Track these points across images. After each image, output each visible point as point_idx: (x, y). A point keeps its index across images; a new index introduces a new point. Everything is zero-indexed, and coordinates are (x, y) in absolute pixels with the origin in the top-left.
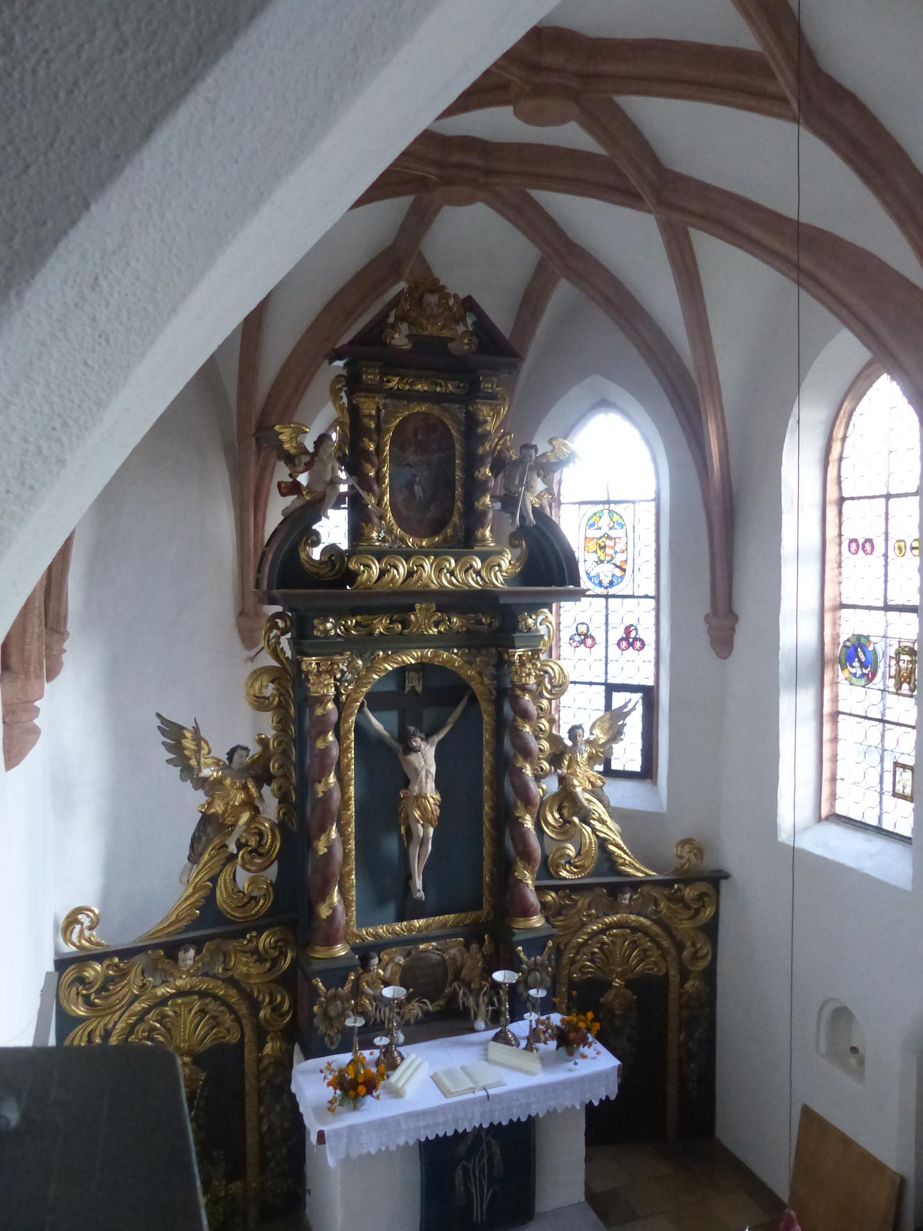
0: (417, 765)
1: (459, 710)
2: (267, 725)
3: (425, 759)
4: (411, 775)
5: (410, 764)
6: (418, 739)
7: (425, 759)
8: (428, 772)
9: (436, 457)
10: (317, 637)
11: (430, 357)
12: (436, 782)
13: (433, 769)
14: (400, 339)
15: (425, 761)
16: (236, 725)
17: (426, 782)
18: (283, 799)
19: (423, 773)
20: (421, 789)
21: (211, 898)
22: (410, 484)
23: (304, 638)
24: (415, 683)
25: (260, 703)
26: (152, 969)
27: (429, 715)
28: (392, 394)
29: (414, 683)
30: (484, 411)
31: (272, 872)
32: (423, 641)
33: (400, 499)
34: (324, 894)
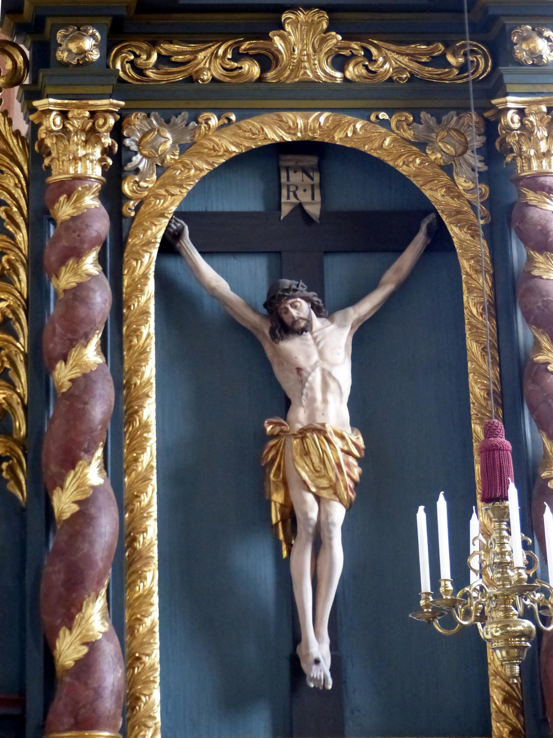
0: (302, 361)
1: (408, 258)
3: (324, 357)
4: (287, 382)
5: (286, 360)
6: (305, 306)
7: (324, 357)
8: (326, 376)
10: (65, 65)
12: (352, 404)
15: (321, 353)
17: (325, 401)
19: (316, 379)
20: (311, 415)
24: (304, 197)
27: (338, 269)
29: (301, 192)
32: (310, 95)
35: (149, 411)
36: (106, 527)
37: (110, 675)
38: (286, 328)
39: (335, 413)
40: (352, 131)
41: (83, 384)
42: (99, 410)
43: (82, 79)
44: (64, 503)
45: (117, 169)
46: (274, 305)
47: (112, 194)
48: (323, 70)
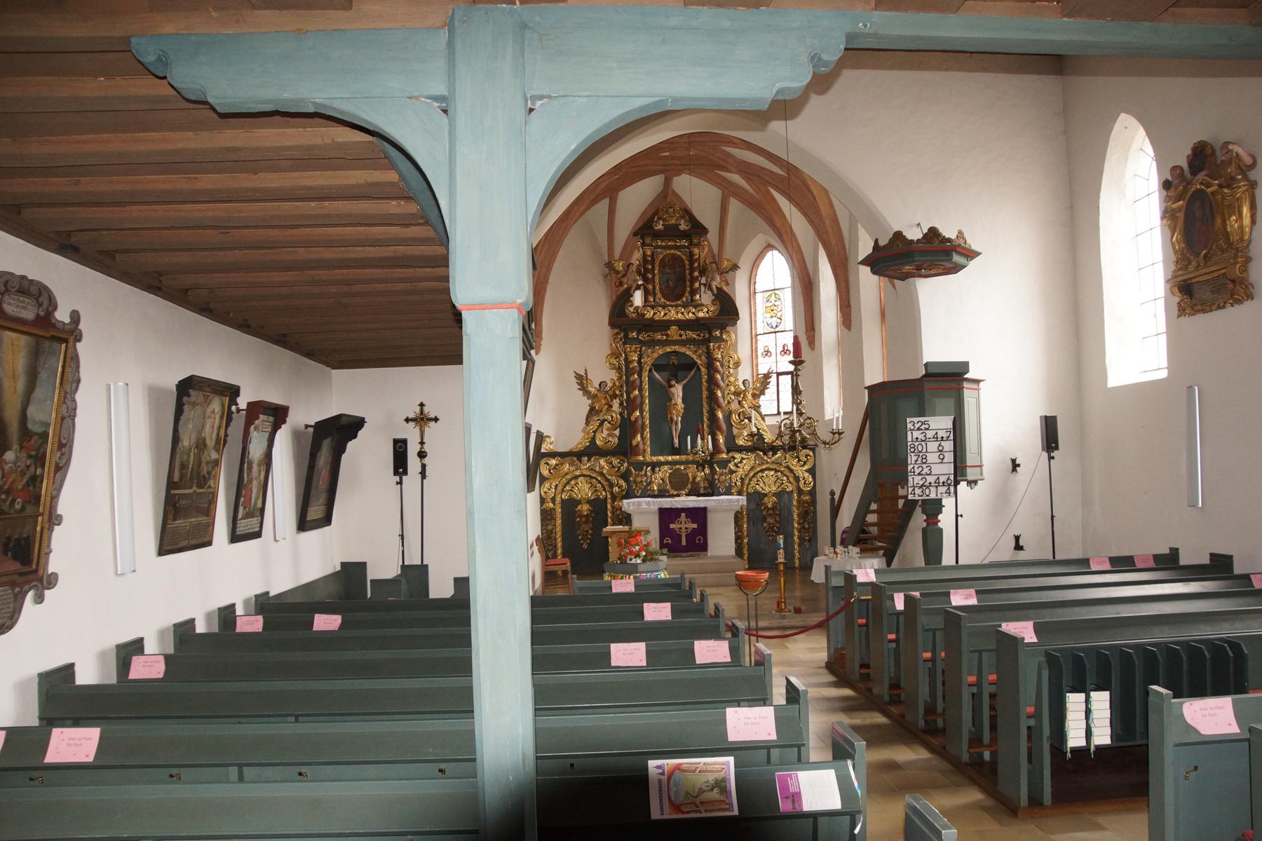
2: (613, 375)
3: (678, 391)
7: (678, 391)
11: (672, 232)
12: (683, 399)
14: (660, 226)
16: (602, 374)
18: (621, 404)
21: (594, 439)
22: (667, 281)
23: (627, 340)
25: (613, 367)
26: (572, 464)
27: (680, 374)
28: (658, 247)
29: (674, 360)
30: (696, 251)
31: (617, 432)
32: (675, 343)
34: (634, 437)
36: (640, 422)
37: (641, 447)
38: (671, 386)
39: (680, 401)
40: (683, 350)
41: (636, 397)
42: (638, 402)
43: (636, 341)
44: (633, 418)
45: (640, 357)
46: (668, 382)
47: (639, 362)
48: (676, 337)
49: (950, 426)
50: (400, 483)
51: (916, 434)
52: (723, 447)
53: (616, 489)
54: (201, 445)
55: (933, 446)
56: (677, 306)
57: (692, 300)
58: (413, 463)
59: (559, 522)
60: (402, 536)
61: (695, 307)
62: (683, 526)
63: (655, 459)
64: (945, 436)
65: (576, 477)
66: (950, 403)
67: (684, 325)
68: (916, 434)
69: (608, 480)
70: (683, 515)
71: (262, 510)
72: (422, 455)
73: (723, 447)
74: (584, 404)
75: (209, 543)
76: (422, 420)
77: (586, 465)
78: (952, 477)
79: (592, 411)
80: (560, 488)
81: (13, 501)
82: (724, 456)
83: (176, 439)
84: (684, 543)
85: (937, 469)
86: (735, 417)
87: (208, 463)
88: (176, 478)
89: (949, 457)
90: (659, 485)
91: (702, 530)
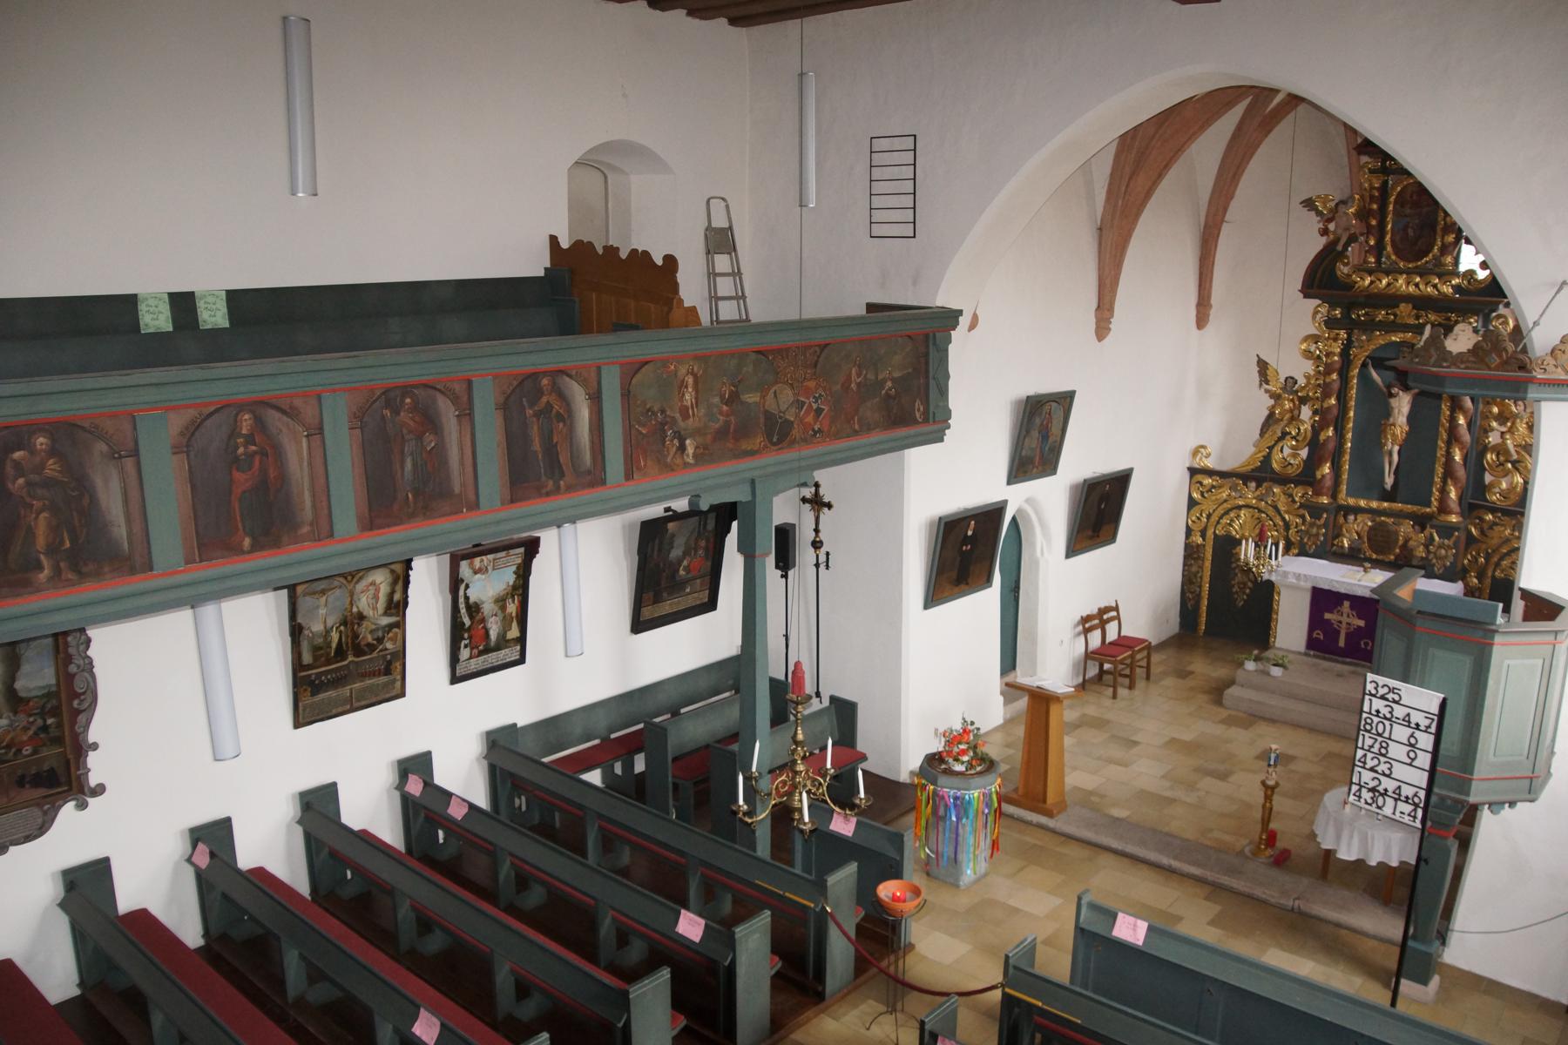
2: (1309, 367)
3: (1402, 405)
7: (1402, 405)
9: (1425, 210)
13: (1406, 409)
21: (1267, 459)
25: (1308, 354)
26: (1233, 488)
31: (1304, 453)
33: (1398, 238)
35: (1352, 414)
38: (1391, 395)
44: (1322, 437)
46: (1389, 387)
49: (1435, 709)
50: (785, 576)
51: (1378, 704)
52: (1454, 506)
53: (1292, 531)
54: (353, 621)
55: (1401, 733)
56: (1409, 272)
57: (1438, 262)
58: (805, 555)
59: (1208, 564)
60: (786, 636)
61: (1440, 276)
62: (1345, 619)
63: (1351, 501)
64: (1424, 723)
65: (1239, 508)
66: (1465, 663)
67: (1422, 303)
68: (1378, 704)
69: (1283, 519)
70: (1347, 604)
71: (522, 640)
72: (817, 545)
73: (1454, 506)
74: (1261, 404)
75: (402, 694)
76: (818, 503)
77: (1250, 494)
78: (1422, 794)
79: (1270, 420)
80: (1214, 518)
81: (19, 751)
82: (1454, 519)
83: (296, 631)
84: (1342, 643)
85: (1400, 771)
86: (1490, 457)
87: (371, 632)
88: (307, 658)
89: (1424, 760)
90: (1351, 541)
91: (1369, 632)
